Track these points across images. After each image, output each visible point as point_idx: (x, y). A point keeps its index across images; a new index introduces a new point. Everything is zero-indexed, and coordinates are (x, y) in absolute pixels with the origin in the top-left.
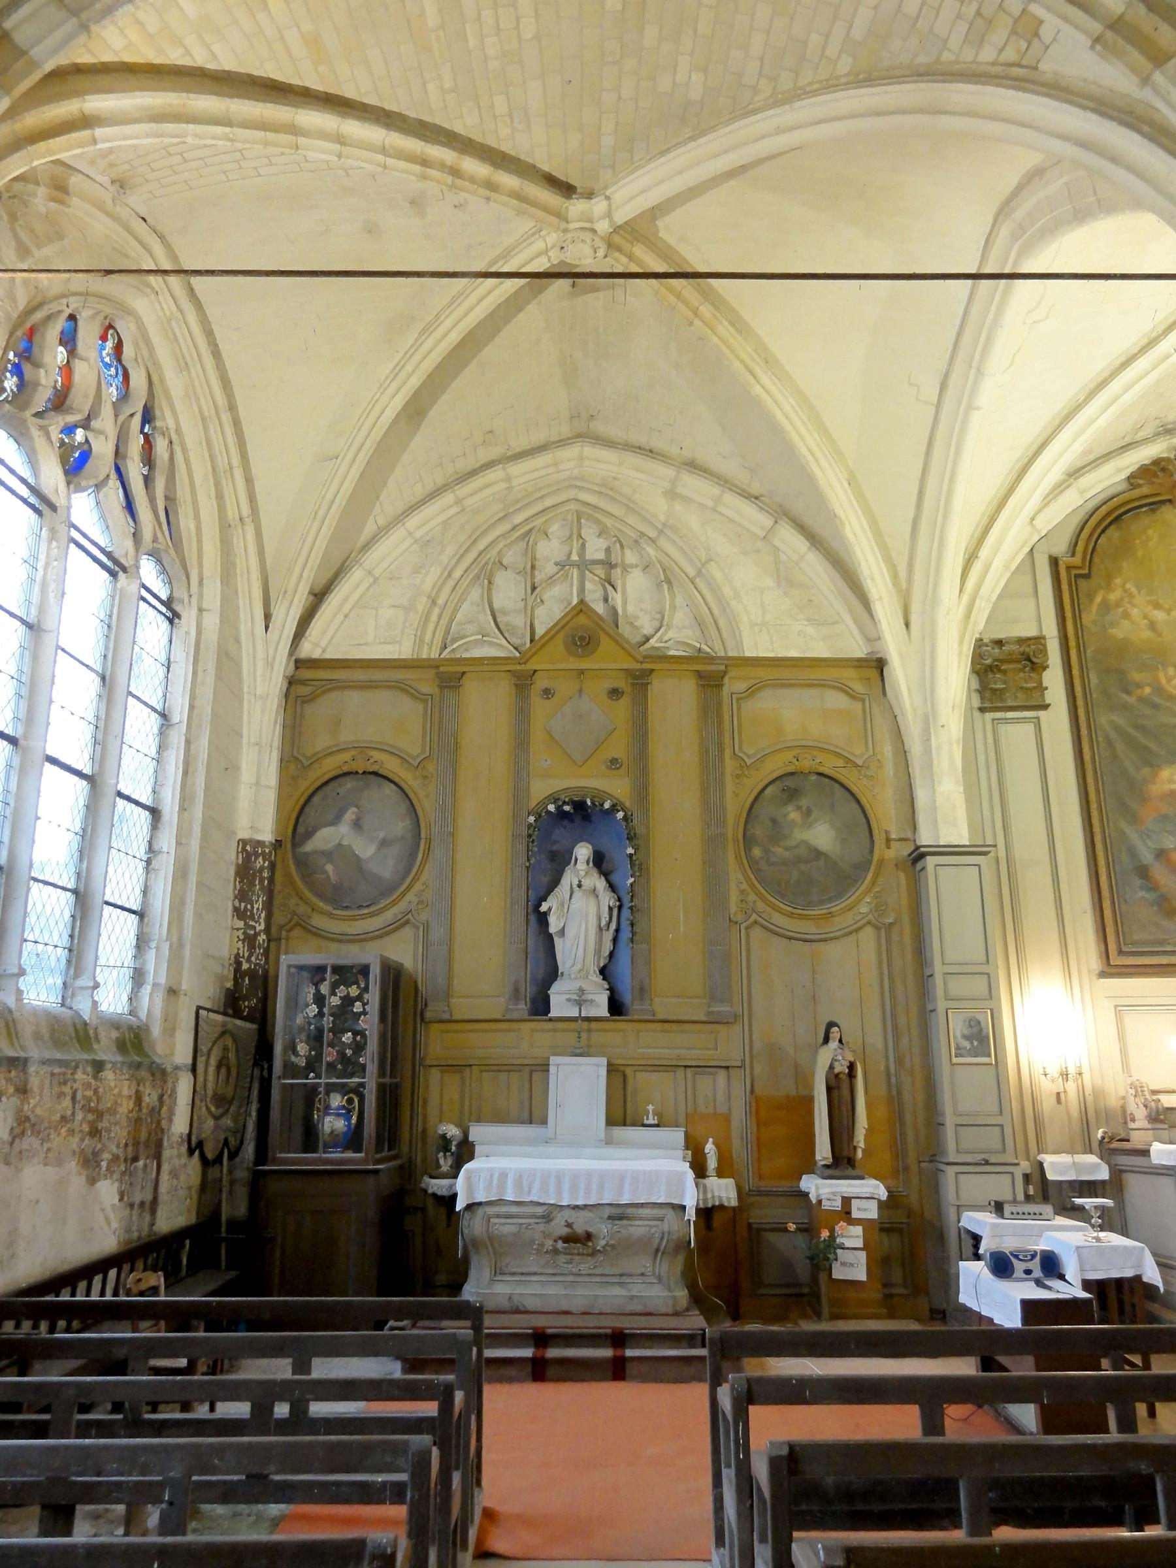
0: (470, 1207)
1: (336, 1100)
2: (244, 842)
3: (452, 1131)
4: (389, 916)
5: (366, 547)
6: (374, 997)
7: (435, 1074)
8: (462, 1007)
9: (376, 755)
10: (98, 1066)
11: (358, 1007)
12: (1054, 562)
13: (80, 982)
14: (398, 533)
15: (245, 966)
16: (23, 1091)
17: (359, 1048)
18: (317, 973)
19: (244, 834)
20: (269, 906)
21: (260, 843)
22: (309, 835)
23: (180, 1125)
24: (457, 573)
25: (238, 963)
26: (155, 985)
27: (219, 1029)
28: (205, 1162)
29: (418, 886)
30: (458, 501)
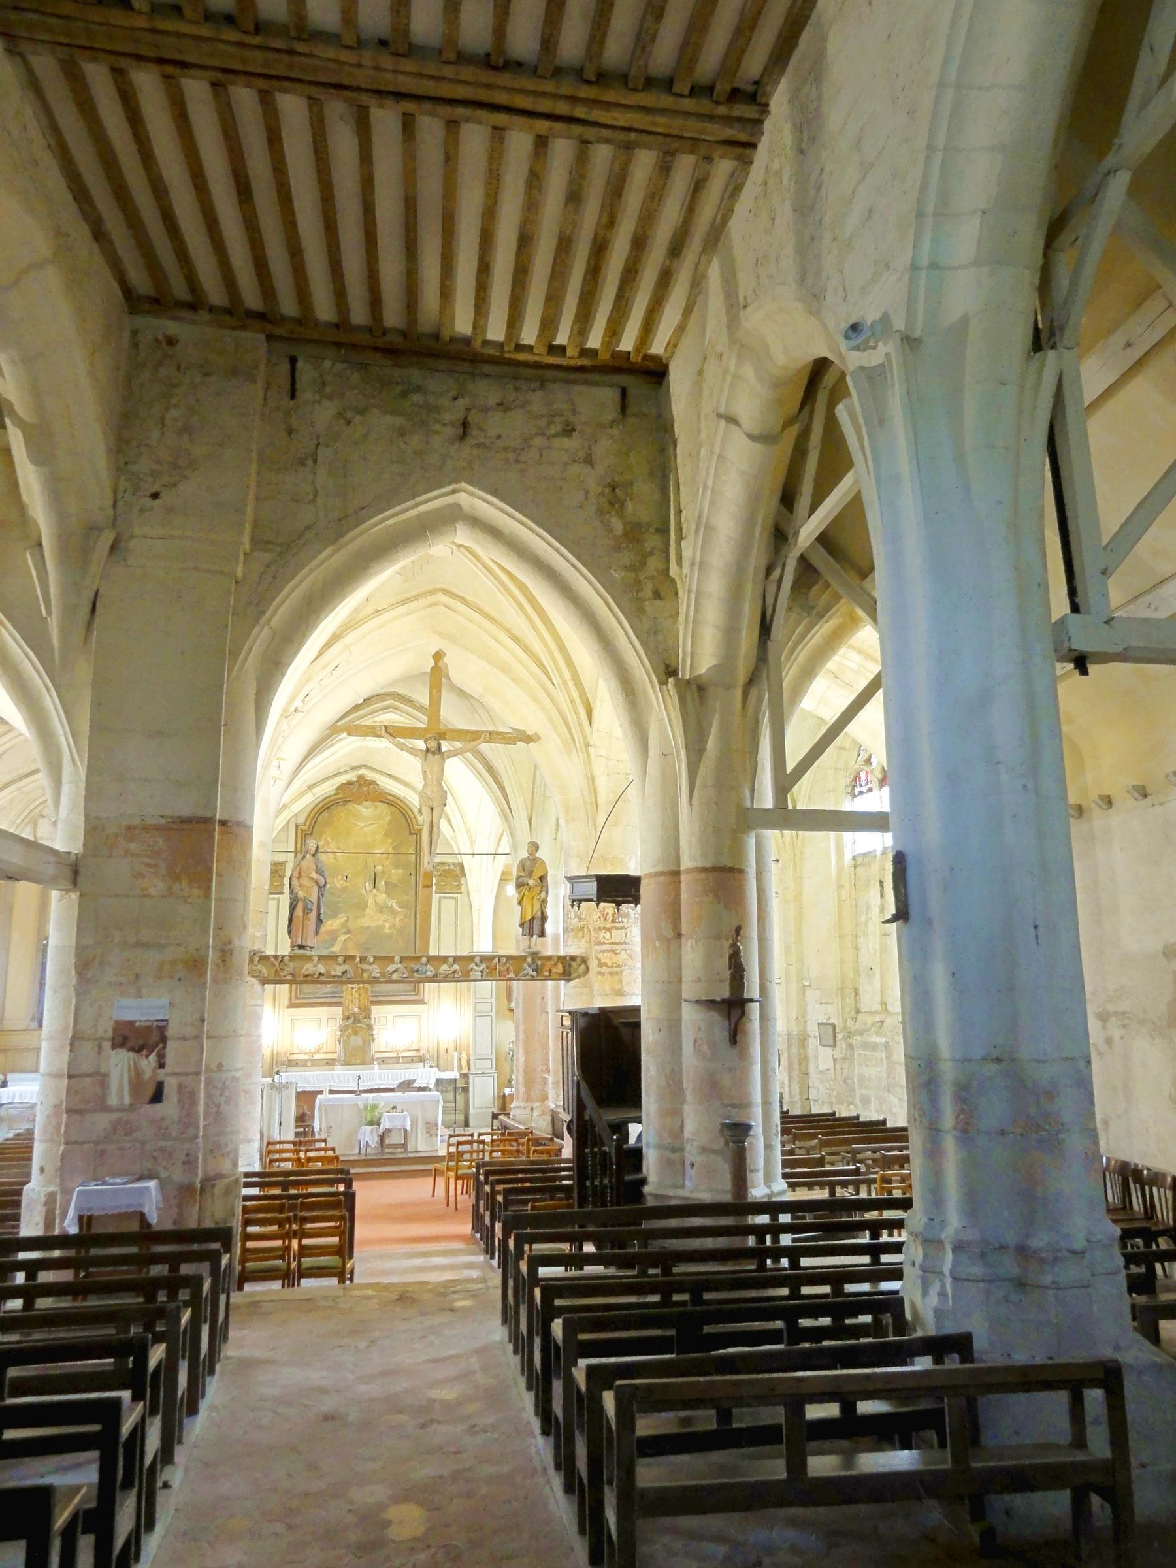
12: (297, 826)
24: (18, 822)
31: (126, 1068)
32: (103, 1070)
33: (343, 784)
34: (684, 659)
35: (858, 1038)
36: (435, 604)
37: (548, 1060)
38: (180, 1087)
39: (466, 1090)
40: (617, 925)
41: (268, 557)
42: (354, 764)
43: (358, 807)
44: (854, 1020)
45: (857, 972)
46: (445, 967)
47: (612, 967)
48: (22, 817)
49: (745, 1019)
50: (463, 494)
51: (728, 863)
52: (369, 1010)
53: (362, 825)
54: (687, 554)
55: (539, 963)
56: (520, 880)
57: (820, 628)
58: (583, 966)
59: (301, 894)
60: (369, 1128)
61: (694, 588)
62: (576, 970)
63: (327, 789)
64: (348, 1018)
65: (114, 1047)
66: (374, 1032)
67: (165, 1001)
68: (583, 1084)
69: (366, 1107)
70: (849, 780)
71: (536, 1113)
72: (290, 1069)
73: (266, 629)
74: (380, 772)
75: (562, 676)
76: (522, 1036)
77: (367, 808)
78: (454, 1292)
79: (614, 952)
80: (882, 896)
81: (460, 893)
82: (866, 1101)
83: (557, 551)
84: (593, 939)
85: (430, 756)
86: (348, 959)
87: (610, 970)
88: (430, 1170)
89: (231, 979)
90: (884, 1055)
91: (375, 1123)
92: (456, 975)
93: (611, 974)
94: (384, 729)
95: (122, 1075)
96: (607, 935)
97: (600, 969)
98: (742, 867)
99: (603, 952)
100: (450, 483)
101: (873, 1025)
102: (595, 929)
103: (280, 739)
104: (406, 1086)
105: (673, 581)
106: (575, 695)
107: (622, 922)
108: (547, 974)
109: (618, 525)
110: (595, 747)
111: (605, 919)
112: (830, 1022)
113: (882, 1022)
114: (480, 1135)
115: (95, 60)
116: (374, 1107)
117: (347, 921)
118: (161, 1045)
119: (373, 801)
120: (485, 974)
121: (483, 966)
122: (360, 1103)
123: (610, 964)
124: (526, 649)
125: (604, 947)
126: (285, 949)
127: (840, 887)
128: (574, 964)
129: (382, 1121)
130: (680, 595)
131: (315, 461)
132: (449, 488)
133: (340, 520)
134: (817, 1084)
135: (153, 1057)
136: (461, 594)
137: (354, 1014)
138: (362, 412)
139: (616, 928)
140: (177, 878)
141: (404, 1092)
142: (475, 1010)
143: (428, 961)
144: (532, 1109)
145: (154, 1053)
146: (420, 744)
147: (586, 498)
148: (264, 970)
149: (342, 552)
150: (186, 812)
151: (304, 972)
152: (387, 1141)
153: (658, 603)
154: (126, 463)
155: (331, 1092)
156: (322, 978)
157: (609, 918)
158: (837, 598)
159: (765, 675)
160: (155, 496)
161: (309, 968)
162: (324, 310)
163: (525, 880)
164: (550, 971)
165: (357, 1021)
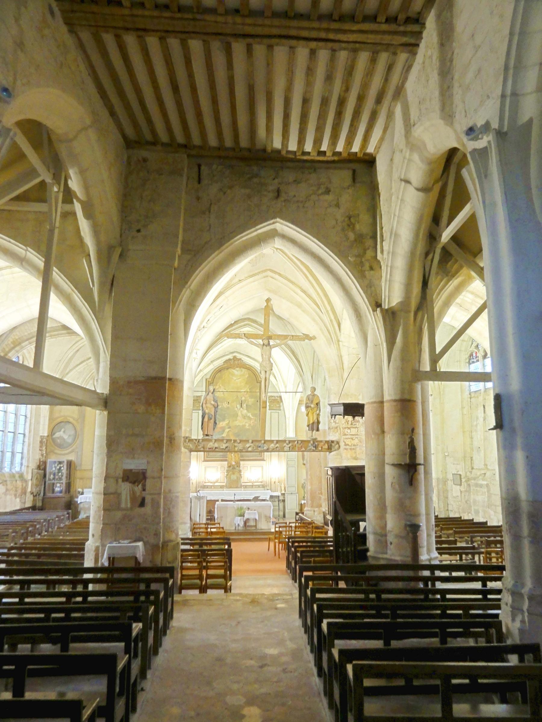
0: (81, 503)
1: (58, 485)
2: (41, 436)
3: (80, 490)
4: (70, 450)
5: (67, 374)
6: (65, 467)
7: (78, 480)
8: (83, 467)
9: (68, 418)
10: (16, 481)
11: (62, 468)
12: (206, 380)
13: (13, 467)
14: (74, 370)
15: (41, 460)
16: (7, 485)
17: (62, 476)
18: (55, 462)
19: (41, 435)
20: (46, 449)
21: (44, 436)
22: (54, 434)
23: (29, 490)
24: (87, 378)
25: (40, 460)
26: (25, 466)
27: (36, 473)
28: (34, 496)
29: (76, 445)
30: (87, 364)
31: (129, 490)
32: (119, 491)
33: (227, 360)
34: (385, 299)
35: (473, 481)
36: (267, 276)
37: (321, 489)
38: (153, 500)
39: (284, 501)
40: (353, 426)
41: (189, 257)
42: (232, 351)
43: (234, 370)
44: (471, 472)
45: (472, 449)
46: (272, 445)
47: (351, 446)
48: (89, 376)
49: (416, 473)
50: (278, 224)
51: (407, 397)
52: (239, 463)
53: (235, 378)
54: (386, 248)
55: (316, 444)
56: (307, 405)
57: (453, 282)
58: (337, 445)
59: (207, 411)
60: (239, 518)
61: (390, 265)
62: (334, 447)
63: (220, 362)
64: (230, 467)
65: (123, 481)
66: (242, 473)
67: (145, 461)
68: (338, 503)
69: (238, 509)
70: (467, 356)
71: (316, 513)
72: (205, 489)
73: (188, 290)
74: (243, 354)
75: (326, 309)
76: (309, 477)
77: (237, 371)
78: (277, 600)
79: (352, 439)
80: (484, 412)
81: (280, 410)
82: (477, 512)
83: (322, 249)
84: (342, 433)
85: (265, 347)
86: (228, 441)
87: (350, 447)
88: (267, 538)
89: (174, 451)
90: (486, 490)
91: (242, 515)
92: (278, 449)
93: (351, 449)
94: (243, 335)
95: (127, 494)
96: (349, 431)
97: (345, 447)
98: (415, 399)
99: (347, 439)
100: (272, 219)
101: (480, 475)
102: (343, 428)
103: (197, 340)
104: (256, 499)
105: (379, 262)
106: (333, 318)
107: (356, 425)
108: (320, 449)
109: (352, 236)
110: (342, 341)
111: (348, 423)
112: (458, 473)
113: (485, 474)
114: (290, 523)
115: (107, 32)
116: (241, 508)
117: (229, 423)
118: (144, 481)
119: (240, 367)
120: (291, 448)
121: (290, 445)
122: (235, 506)
123: (350, 445)
124: (309, 296)
125: (347, 437)
126: (201, 437)
127: (463, 408)
128: (333, 444)
129: (245, 515)
130: (382, 268)
131: (210, 212)
132: (271, 221)
133: (221, 239)
134: (452, 503)
135: (140, 486)
136: (278, 271)
137: (233, 466)
138: (231, 187)
139: (353, 428)
140: (150, 405)
141: (255, 501)
142: (287, 464)
143: (265, 443)
144: (314, 511)
145: (140, 485)
146: (260, 341)
147: (337, 223)
148: (191, 445)
149: (223, 253)
150: (153, 374)
151: (209, 446)
152: (248, 524)
153: (372, 272)
154: (126, 217)
155: (222, 500)
156: (217, 450)
157: (350, 423)
158: (461, 267)
159: (425, 305)
160: (139, 231)
161: (211, 445)
162: (213, 141)
163: (309, 405)
164: (322, 448)
165: (234, 468)
